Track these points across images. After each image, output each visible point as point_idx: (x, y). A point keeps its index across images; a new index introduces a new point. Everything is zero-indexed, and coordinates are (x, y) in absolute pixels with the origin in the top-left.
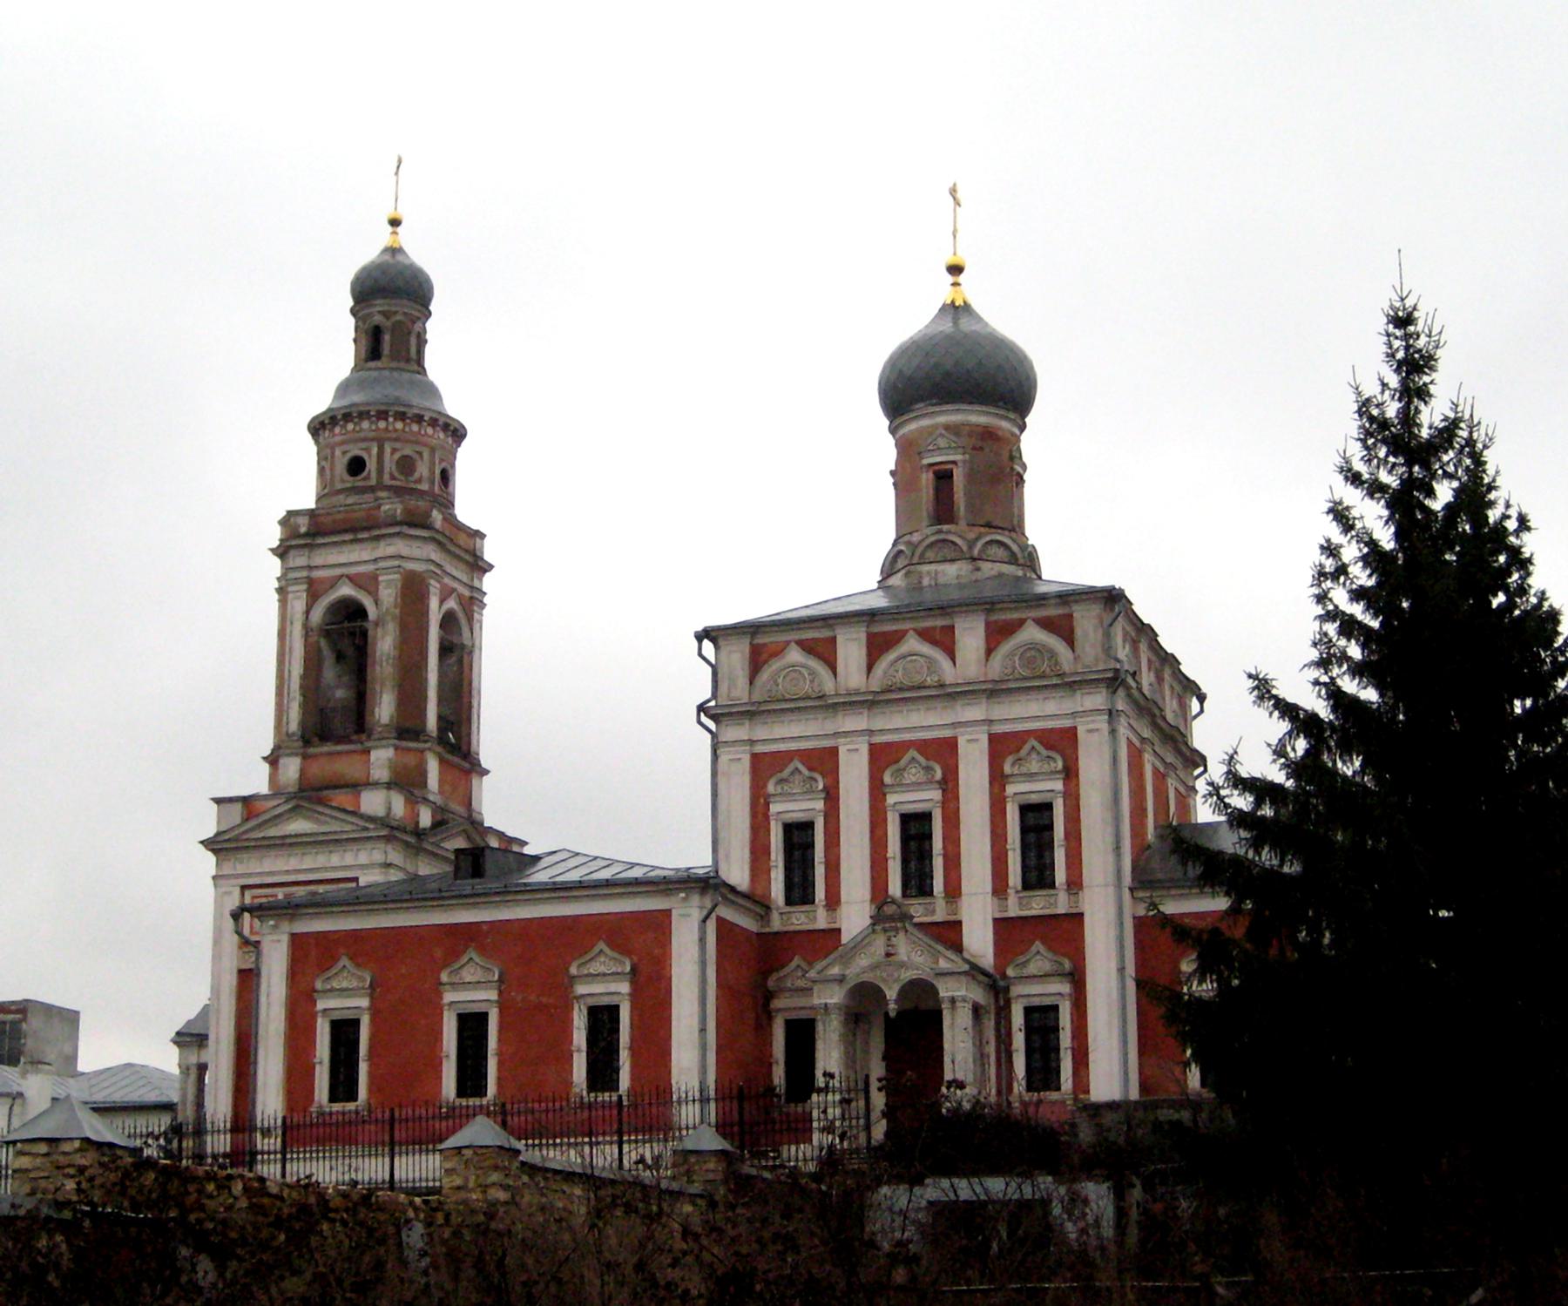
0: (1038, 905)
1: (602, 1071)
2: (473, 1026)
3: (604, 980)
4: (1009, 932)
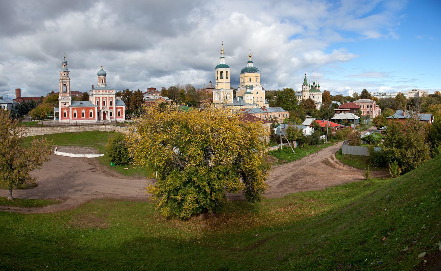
0: (111, 106)
1: (91, 116)
2: (83, 113)
3: (91, 111)
4: (110, 108)
